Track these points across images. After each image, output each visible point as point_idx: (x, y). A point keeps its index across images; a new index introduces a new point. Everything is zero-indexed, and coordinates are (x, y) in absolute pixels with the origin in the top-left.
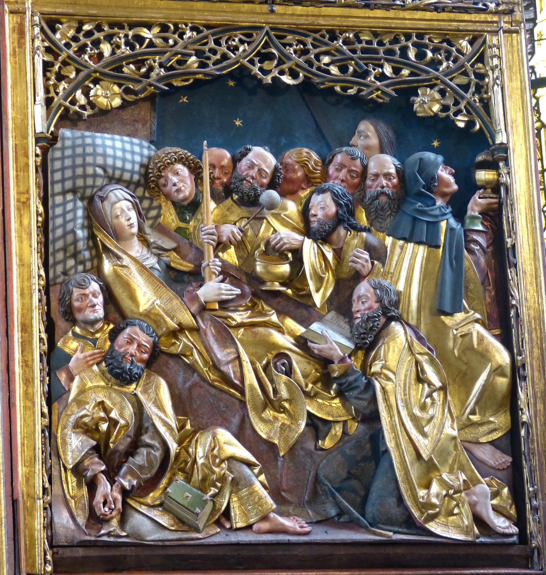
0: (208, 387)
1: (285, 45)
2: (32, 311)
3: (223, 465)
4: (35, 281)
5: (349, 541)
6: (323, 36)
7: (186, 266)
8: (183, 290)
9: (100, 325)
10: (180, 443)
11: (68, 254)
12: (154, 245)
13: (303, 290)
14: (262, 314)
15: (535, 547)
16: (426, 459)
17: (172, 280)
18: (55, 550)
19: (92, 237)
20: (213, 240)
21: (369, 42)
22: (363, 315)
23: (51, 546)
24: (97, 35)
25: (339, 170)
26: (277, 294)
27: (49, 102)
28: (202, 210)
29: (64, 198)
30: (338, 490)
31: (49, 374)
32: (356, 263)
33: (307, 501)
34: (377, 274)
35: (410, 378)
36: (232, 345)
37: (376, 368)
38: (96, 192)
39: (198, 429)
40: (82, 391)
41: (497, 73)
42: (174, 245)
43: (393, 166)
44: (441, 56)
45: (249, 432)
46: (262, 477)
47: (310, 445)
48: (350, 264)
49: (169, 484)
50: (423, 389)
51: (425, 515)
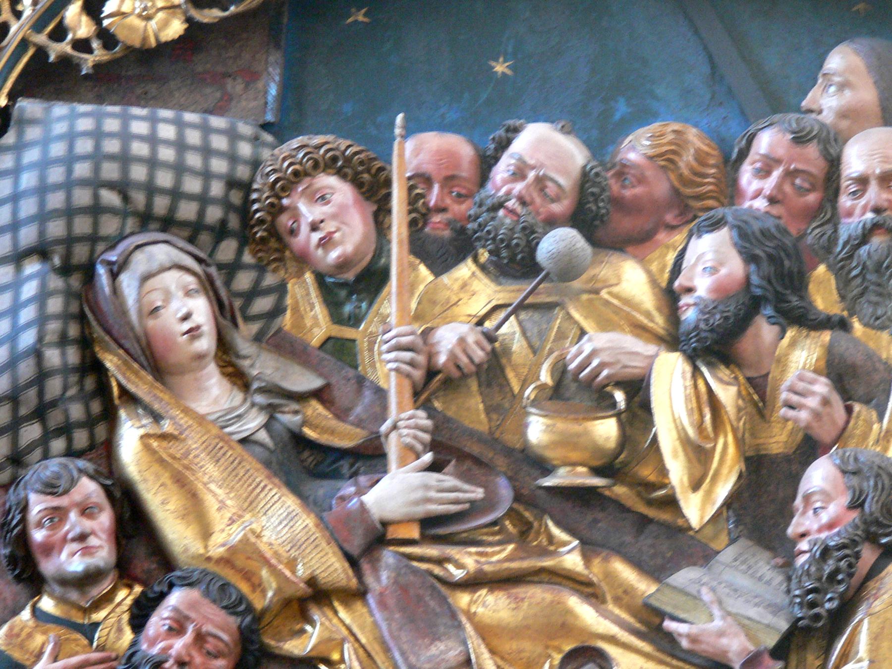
13: (663, 486)
25: (764, 172)
42: (312, 382)
48: (783, 411)
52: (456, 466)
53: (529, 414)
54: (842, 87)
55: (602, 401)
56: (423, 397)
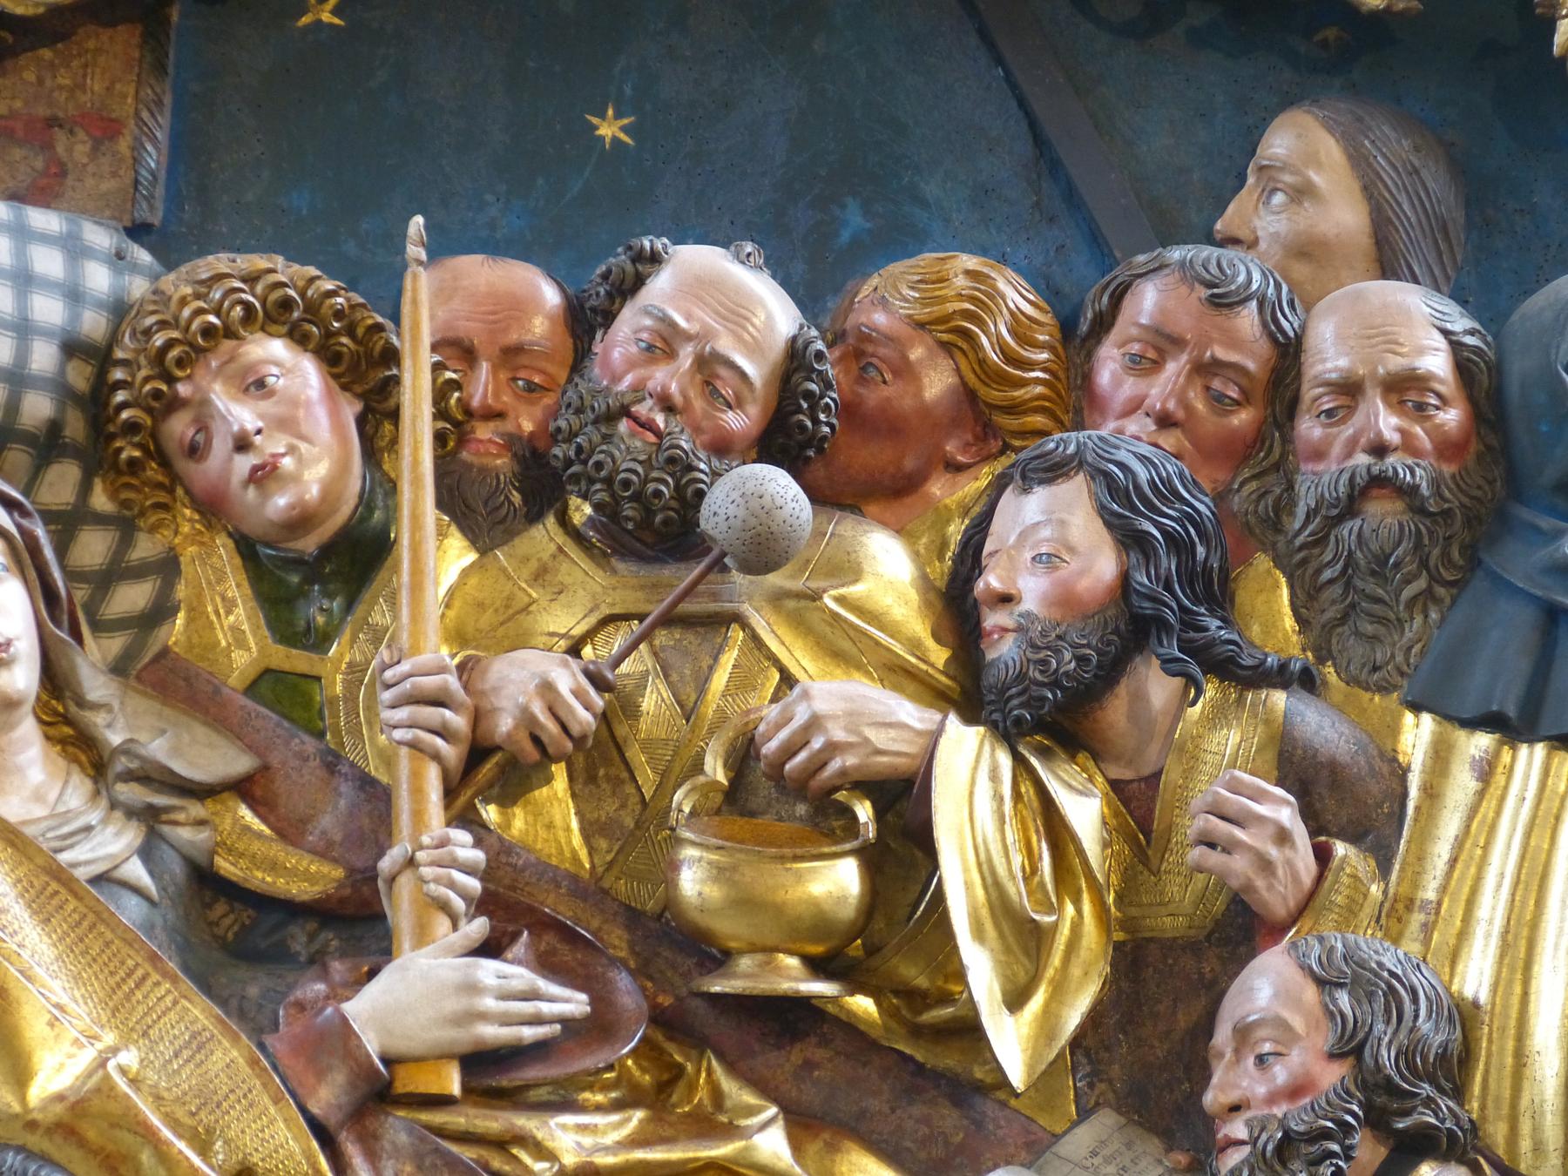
12: (122, 763)
13: (946, 999)
14: (710, 1125)
20: (443, 732)
25: (1144, 365)
26: (788, 1018)
32: (1229, 847)
34: (1351, 911)
42: (236, 763)
43: (1440, 342)
48: (1196, 854)
52: (528, 946)
53: (680, 842)
55: (825, 820)
56: (462, 800)
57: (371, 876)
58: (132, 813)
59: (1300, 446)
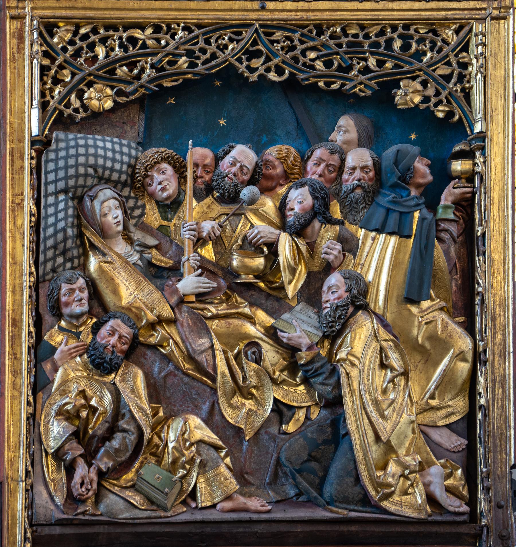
0: (182, 376)
1: (272, 42)
2: (22, 307)
3: (193, 449)
4: (26, 278)
5: (306, 519)
6: (310, 31)
7: (166, 262)
8: (163, 285)
9: (84, 318)
10: (153, 429)
11: (58, 252)
15: (485, 525)
16: (385, 441)
17: (152, 275)
18: (34, 528)
19: (80, 235)
21: (356, 36)
22: (332, 305)
23: (31, 525)
24: (93, 38)
25: (318, 165)
27: (44, 106)
28: (184, 208)
29: (57, 198)
30: (299, 471)
31: (35, 366)
33: (268, 484)
35: (374, 364)
36: (207, 336)
37: (342, 354)
38: (86, 192)
39: (170, 416)
40: (65, 381)
41: (481, 61)
44: (426, 46)
45: (217, 417)
46: (228, 460)
47: (274, 430)
49: (140, 467)
50: (385, 374)
51: (380, 494)
54: (345, 132)
57: (180, 261)
58: (138, 252)
59: (343, 180)
